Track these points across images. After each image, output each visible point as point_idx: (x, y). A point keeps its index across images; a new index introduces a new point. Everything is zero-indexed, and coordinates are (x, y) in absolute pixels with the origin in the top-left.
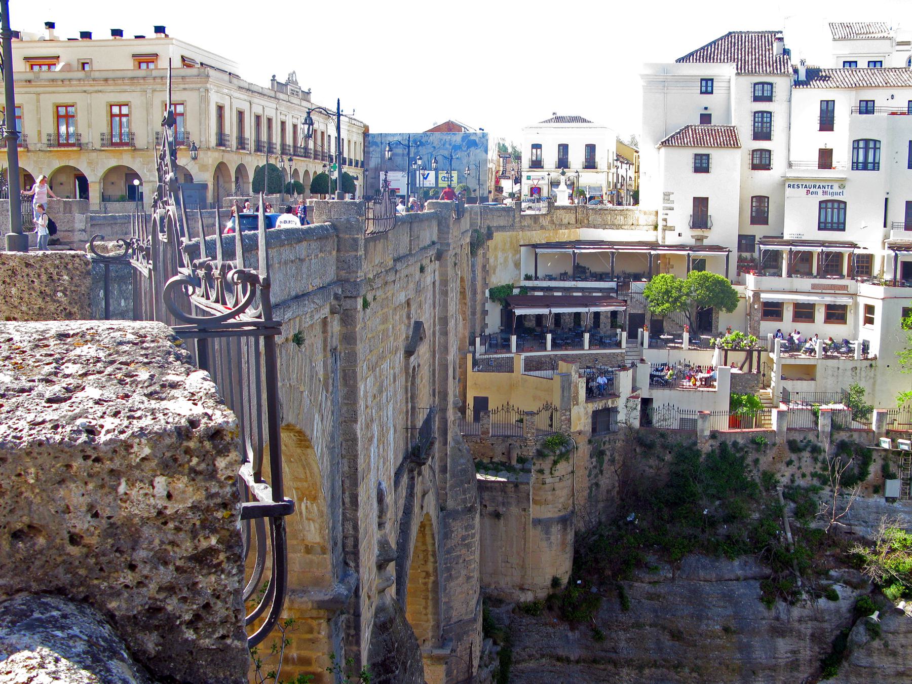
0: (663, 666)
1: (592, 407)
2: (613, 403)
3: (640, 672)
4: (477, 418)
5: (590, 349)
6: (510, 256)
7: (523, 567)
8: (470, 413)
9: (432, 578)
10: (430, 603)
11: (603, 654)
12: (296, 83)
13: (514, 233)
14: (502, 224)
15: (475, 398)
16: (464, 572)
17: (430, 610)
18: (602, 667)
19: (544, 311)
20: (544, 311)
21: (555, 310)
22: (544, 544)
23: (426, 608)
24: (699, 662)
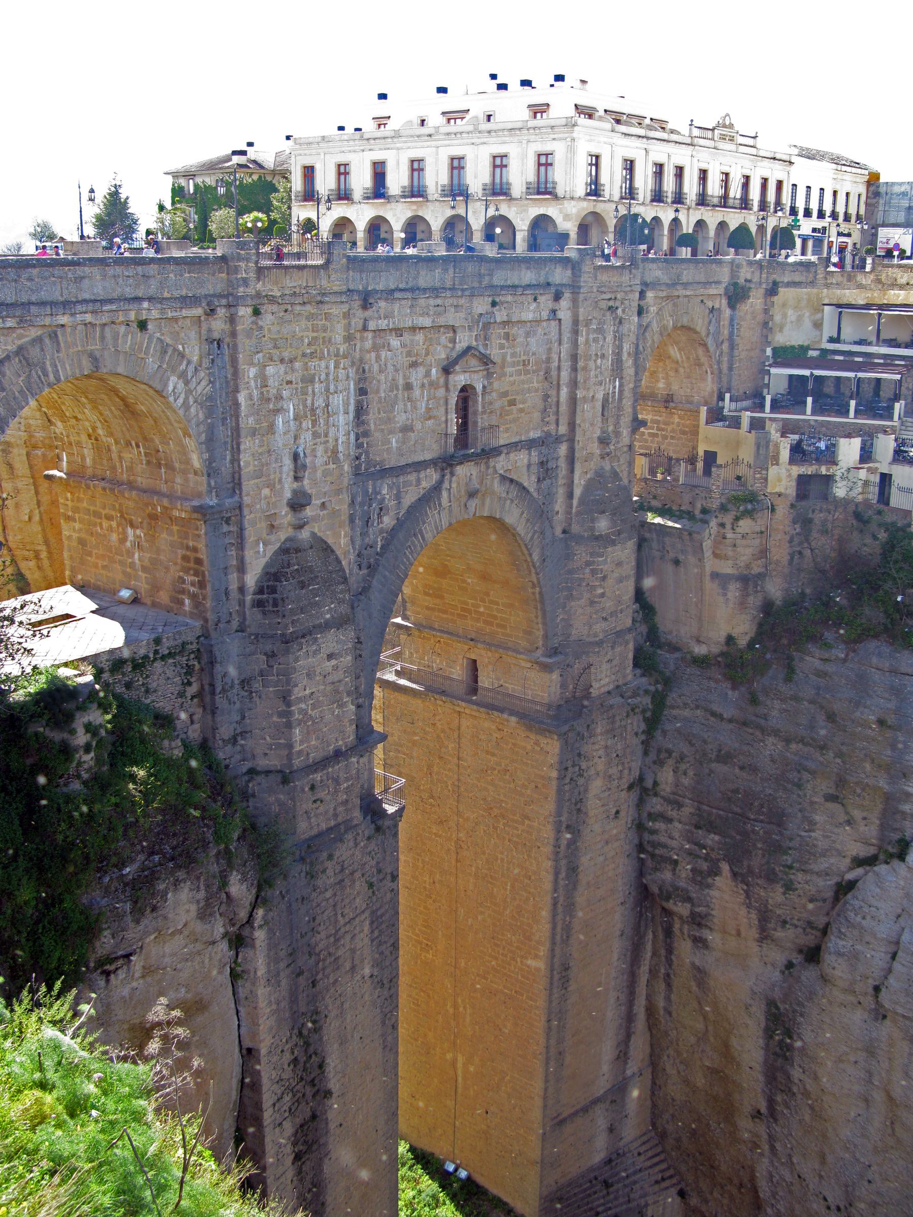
0: (810, 745)
1: (796, 470)
2: (828, 470)
3: (787, 745)
4: (707, 472)
5: (855, 418)
6: (807, 314)
7: (700, 619)
8: (700, 465)
9: (538, 589)
10: (540, 613)
11: (754, 718)
12: (731, 126)
13: (815, 291)
14: (797, 279)
15: (706, 452)
16: (586, 595)
17: (540, 620)
18: (751, 731)
19: (806, 372)
20: (806, 372)
21: (817, 372)
22: (721, 599)
23: (537, 617)
24: (844, 749)
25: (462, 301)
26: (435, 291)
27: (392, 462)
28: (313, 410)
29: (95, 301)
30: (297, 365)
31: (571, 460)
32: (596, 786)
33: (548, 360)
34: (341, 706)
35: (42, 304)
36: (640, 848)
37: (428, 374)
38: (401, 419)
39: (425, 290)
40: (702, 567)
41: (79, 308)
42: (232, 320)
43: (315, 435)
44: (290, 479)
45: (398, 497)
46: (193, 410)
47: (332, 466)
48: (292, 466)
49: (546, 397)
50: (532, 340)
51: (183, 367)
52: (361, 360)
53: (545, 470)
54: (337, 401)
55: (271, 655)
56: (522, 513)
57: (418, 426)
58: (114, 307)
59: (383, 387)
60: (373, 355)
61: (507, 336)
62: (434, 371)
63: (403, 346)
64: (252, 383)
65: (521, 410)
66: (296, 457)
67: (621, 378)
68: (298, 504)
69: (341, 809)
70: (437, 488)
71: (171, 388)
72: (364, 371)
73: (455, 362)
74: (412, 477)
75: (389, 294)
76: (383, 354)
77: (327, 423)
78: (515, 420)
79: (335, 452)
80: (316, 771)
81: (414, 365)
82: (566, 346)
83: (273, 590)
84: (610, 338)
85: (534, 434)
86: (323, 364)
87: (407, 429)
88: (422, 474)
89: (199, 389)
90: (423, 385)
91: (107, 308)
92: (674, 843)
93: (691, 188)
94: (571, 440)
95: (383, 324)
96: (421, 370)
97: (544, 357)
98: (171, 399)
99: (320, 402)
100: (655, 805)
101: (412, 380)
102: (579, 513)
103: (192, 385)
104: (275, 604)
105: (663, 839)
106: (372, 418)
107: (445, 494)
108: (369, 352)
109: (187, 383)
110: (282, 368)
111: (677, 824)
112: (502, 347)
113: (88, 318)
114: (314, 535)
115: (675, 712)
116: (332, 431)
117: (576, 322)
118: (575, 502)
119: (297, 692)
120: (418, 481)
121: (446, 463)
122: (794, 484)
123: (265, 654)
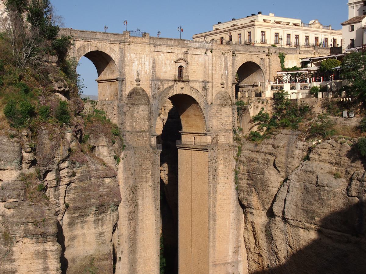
13: (297, 55)
14: (291, 52)
25: (179, 48)
26: (172, 46)
27: (162, 78)
28: (141, 64)
29: (98, 39)
30: (138, 55)
31: (212, 87)
32: (221, 167)
33: (205, 64)
34: (145, 121)
35: (89, 38)
36: (237, 189)
37: (171, 62)
38: (164, 70)
39: (169, 45)
40: (250, 116)
41: (95, 39)
42: (125, 45)
43: (142, 69)
44: (136, 76)
45: (163, 85)
46: (116, 60)
47: (145, 75)
48: (136, 73)
49: (205, 72)
50: (200, 60)
51: (115, 52)
52: (154, 57)
53: (205, 88)
54: (147, 63)
55: (129, 107)
56: (197, 96)
57: (168, 72)
58: (102, 40)
59: (159, 63)
60: (157, 56)
61: (192, 57)
62: (172, 62)
63: (164, 55)
64: (128, 57)
65: (197, 74)
66: (137, 72)
67: (227, 70)
68: (138, 81)
69: (144, 143)
70: (173, 86)
71: (112, 55)
72: (154, 59)
73: (177, 61)
74: (167, 82)
75: (160, 45)
76: (159, 57)
77: (144, 67)
78: (195, 76)
79: (146, 73)
80: (138, 133)
81: (167, 59)
82: (210, 61)
83: (131, 95)
84: (223, 61)
85: (202, 80)
86: (144, 55)
87: (165, 72)
88: (169, 82)
89: (118, 56)
90: (169, 64)
91: (100, 40)
92: (243, 185)
93: (302, 42)
94: (212, 83)
95: (159, 50)
96: (169, 61)
97: (204, 63)
98: (112, 57)
99: (143, 62)
100: (240, 176)
101: (167, 63)
102: (214, 99)
103: (116, 55)
104: (131, 97)
105: (241, 185)
106: (157, 69)
107: (175, 87)
108: (156, 55)
109: (115, 55)
110: (135, 55)
111: (244, 180)
112: (191, 59)
113: (97, 41)
114: (141, 87)
115: (243, 151)
116: (146, 69)
117: (212, 56)
118: (214, 97)
119: (135, 115)
120: (168, 84)
121: (175, 81)
122: (272, 95)
123: (129, 107)
